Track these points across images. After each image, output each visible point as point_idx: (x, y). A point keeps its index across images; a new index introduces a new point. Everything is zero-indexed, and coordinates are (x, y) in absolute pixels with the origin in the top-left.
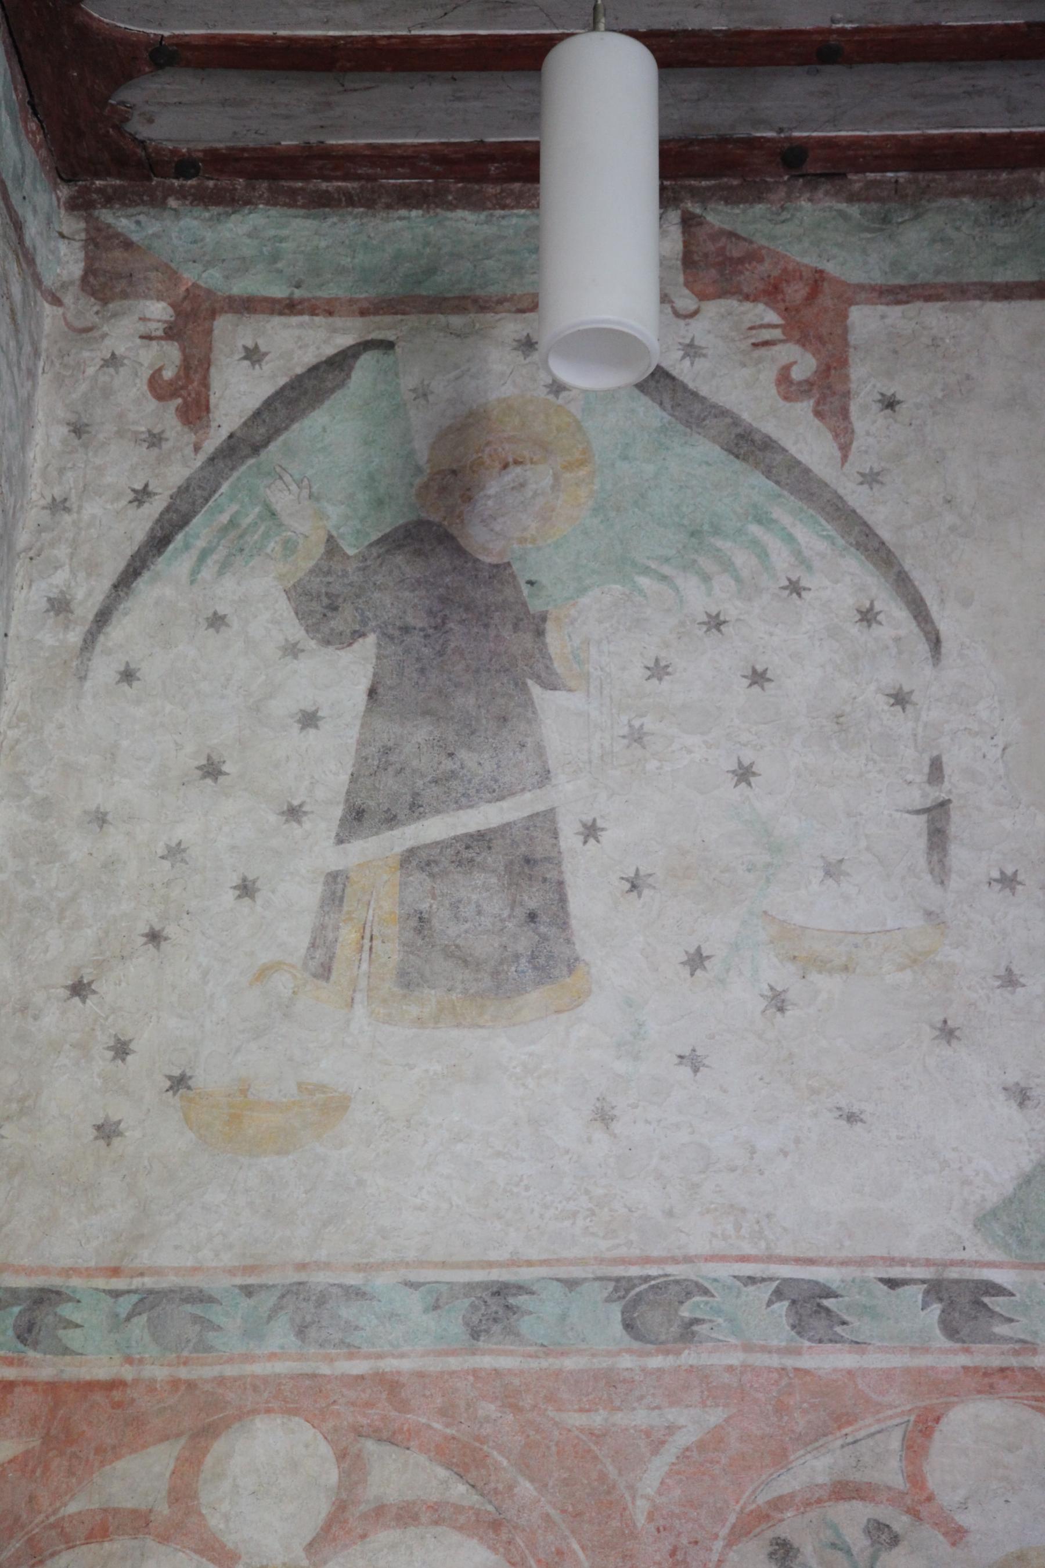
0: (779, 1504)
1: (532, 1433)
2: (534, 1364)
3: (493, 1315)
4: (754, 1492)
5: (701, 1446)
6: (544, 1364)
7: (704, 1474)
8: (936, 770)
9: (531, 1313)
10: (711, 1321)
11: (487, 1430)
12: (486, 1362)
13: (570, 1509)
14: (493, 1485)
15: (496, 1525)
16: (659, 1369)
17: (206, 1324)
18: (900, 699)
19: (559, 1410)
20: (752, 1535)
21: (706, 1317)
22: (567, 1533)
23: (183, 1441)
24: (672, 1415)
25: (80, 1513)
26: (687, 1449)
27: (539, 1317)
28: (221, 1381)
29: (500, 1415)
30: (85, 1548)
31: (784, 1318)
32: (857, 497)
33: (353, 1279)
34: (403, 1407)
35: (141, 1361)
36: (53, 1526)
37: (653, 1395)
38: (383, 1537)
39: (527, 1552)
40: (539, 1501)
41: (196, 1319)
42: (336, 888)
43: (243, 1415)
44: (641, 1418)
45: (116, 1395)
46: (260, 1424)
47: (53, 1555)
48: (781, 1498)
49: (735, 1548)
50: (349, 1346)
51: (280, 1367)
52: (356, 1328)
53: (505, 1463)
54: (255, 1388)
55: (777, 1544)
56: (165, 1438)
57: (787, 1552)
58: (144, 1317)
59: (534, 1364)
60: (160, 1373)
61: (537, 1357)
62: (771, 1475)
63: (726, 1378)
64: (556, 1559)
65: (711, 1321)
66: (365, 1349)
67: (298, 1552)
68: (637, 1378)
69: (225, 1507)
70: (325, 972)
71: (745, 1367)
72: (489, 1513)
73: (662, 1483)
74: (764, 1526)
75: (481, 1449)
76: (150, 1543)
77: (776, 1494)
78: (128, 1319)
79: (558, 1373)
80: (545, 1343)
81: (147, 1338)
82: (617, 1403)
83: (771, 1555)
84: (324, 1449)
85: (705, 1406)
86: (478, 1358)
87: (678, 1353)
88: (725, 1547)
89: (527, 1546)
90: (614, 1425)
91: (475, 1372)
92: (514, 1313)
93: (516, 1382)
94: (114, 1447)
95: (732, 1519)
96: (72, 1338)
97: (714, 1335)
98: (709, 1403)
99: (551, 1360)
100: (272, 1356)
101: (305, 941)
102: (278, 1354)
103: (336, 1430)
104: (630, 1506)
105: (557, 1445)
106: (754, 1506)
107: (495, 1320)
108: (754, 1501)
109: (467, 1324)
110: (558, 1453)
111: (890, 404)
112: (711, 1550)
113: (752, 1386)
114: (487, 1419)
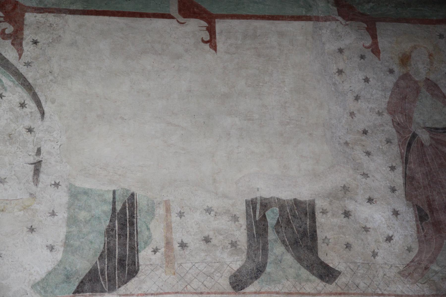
8: (39, 152)
18: (30, 130)
32: (23, 69)
111: (35, 42)
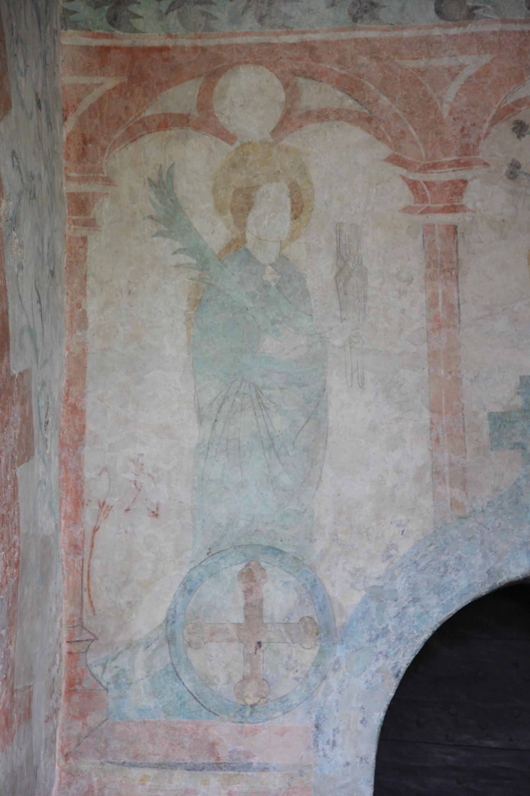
0: (519, 103)
1: (387, 72)
2: (387, 35)
3: (365, 8)
4: (505, 97)
5: (477, 75)
6: (393, 34)
7: (479, 89)
9: (385, 7)
10: (484, 7)
11: (363, 71)
12: (361, 34)
13: (408, 110)
14: (367, 100)
15: (369, 120)
16: (455, 35)
19: (401, 59)
20: (504, 120)
21: (481, 5)
22: (407, 122)
23: (202, 79)
24: (462, 59)
25: (152, 115)
26: (470, 77)
27: (389, 9)
28: (220, 47)
29: (369, 62)
30: (157, 133)
31: (524, 3)
34: (318, 59)
35: (176, 36)
36: (139, 122)
37: (452, 49)
38: (310, 127)
39: (386, 133)
40: (391, 107)
41: (203, 13)
43: (233, 65)
44: (445, 61)
45: (165, 54)
46: (242, 70)
47: (141, 136)
48: (520, 100)
49: (495, 126)
50: (287, 27)
51: (250, 39)
52: (290, 17)
53: (373, 88)
54: (238, 51)
55: (517, 123)
57: (522, 127)
58: (176, 12)
59: (387, 35)
60: (187, 43)
61: (389, 31)
62: (515, 88)
63: (492, 38)
64: (401, 136)
65: (484, 7)
66: (296, 29)
67: (267, 135)
68: (443, 40)
69: (227, 113)
71: (502, 32)
72: (366, 114)
73: (457, 95)
74: (510, 115)
75: (360, 81)
76: (190, 131)
77: (517, 98)
78: (167, 13)
79: (400, 40)
80: (393, 23)
81: (178, 24)
82: (432, 54)
83: (514, 129)
84: (277, 82)
85: (479, 53)
86: (357, 32)
87: (465, 26)
88: (489, 126)
89: (386, 129)
90: (430, 66)
91: (356, 40)
92: (376, 7)
93: (378, 45)
94: (166, 82)
95: (494, 111)
96: (138, 23)
97: (485, 15)
98: (482, 52)
99: (396, 32)
100: (246, 34)
103: (282, 72)
104: (440, 107)
105: (400, 77)
106: (505, 105)
107: (366, 11)
108: (505, 102)
109: (350, 14)
110: (401, 82)
112: (482, 128)
113: (505, 42)
114: (363, 65)
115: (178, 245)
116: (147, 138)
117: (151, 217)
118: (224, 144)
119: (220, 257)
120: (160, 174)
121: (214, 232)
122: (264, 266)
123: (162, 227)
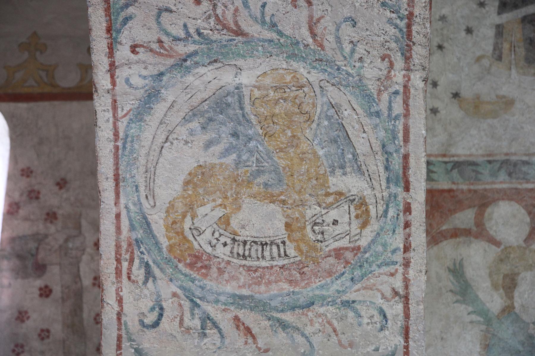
17: (477, 172)
23: (476, 208)
25: (447, 229)
28: (485, 190)
30: (451, 240)
33: (525, 158)
35: (458, 184)
36: (439, 233)
41: (473, 171)
42: (500, 30)
43: (495, 201)
45: (452, 194)
46: (501, 203)
47: (441, 241)
50: (526, 179)
51: (505, 186)
52: (528, 174)
54: (497, 192)
56: (470, 207)
58: (456, 170)
60: (465, 187)
66: (532, 180)
69: (494, 228)
70: (500, 58)
76: (472, 239)
78: (451, 170)
81: (458, 177)
84: (523, 211)
94: (454, 210)
100: (501, 182)
101: (491, 48)
102: (503, 182)
103: (526, 205)
115: (470, 309)
116: (445, 243)
117: (451, 291)
118: (494, 247)
119: (498, 317)
120: (455, 264)
121: (495, 302)
122: (528, 324)
123: (459, 297)
